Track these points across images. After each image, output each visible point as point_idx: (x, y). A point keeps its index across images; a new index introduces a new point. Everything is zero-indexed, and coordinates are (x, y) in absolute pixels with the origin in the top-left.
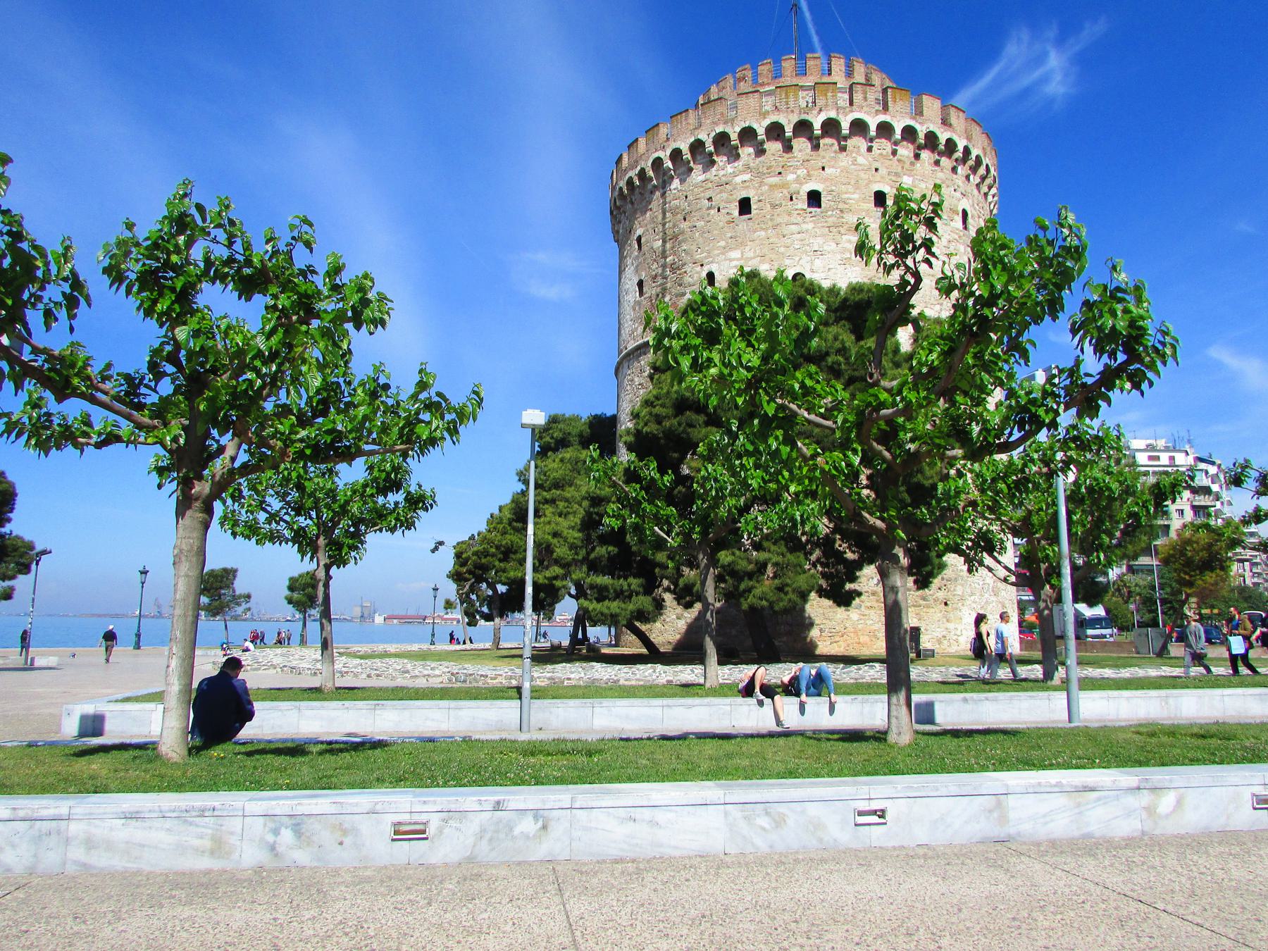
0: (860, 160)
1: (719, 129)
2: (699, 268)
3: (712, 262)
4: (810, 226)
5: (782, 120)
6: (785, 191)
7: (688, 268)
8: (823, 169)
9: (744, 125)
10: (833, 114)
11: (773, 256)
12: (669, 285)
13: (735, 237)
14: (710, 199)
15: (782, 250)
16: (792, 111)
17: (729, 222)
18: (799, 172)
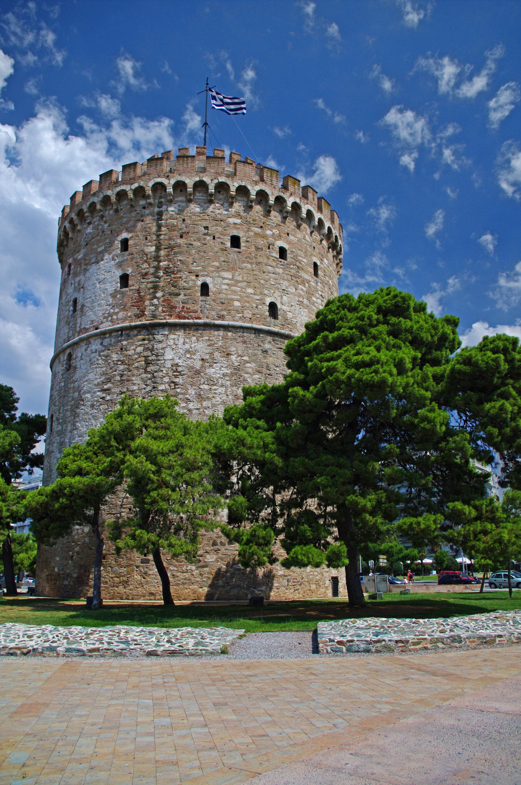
0: (307, 237)
1: (222, 179)
2: (194, 278)
3: (207, 276)
4: (281, 271)
6: (265, 241)
7: (184, 275)
8: (288, 234)
9: (243, 184)
10: (298, 201)
11: (257, 285)
12: (161, 284)
13: (228, 262)
14: (206, 228)
15: (262, 282)
16: (275, 188)
17: (222, 250)
18: (274, 231)
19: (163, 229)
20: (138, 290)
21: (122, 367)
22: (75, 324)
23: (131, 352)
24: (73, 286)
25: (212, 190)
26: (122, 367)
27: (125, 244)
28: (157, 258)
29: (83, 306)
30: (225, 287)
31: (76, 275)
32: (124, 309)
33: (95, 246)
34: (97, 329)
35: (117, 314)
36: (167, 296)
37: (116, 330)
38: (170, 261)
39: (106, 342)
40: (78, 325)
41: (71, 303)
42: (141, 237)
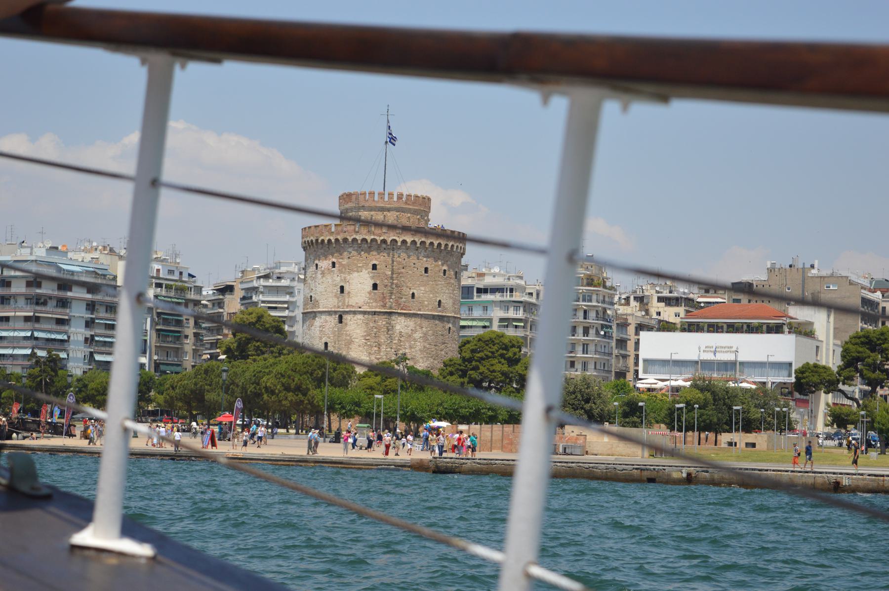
4: (443, 283)
5: (442, 243)
14: (414, 264)
19: (395, 263)
20: (383, 294)
21: (375, 330)
22: (344, 302)
23: (380, 324)
24: (339, 277)
25: (418, 245)
26: (375, 330)
27: (374, 267)
28: (392, 278)
29: (349, 293)
30: (421, 295)
31: (340, 271)
32: (376, 301)
33: (355, 262)
34: (360, 308)
35: (372, 303)
36: (397, 298)
37: (372, 312)
38: (398, 280)
39: (366, 316)
40: (347, 302)
41: (339, 287)
42: (384, 264)
